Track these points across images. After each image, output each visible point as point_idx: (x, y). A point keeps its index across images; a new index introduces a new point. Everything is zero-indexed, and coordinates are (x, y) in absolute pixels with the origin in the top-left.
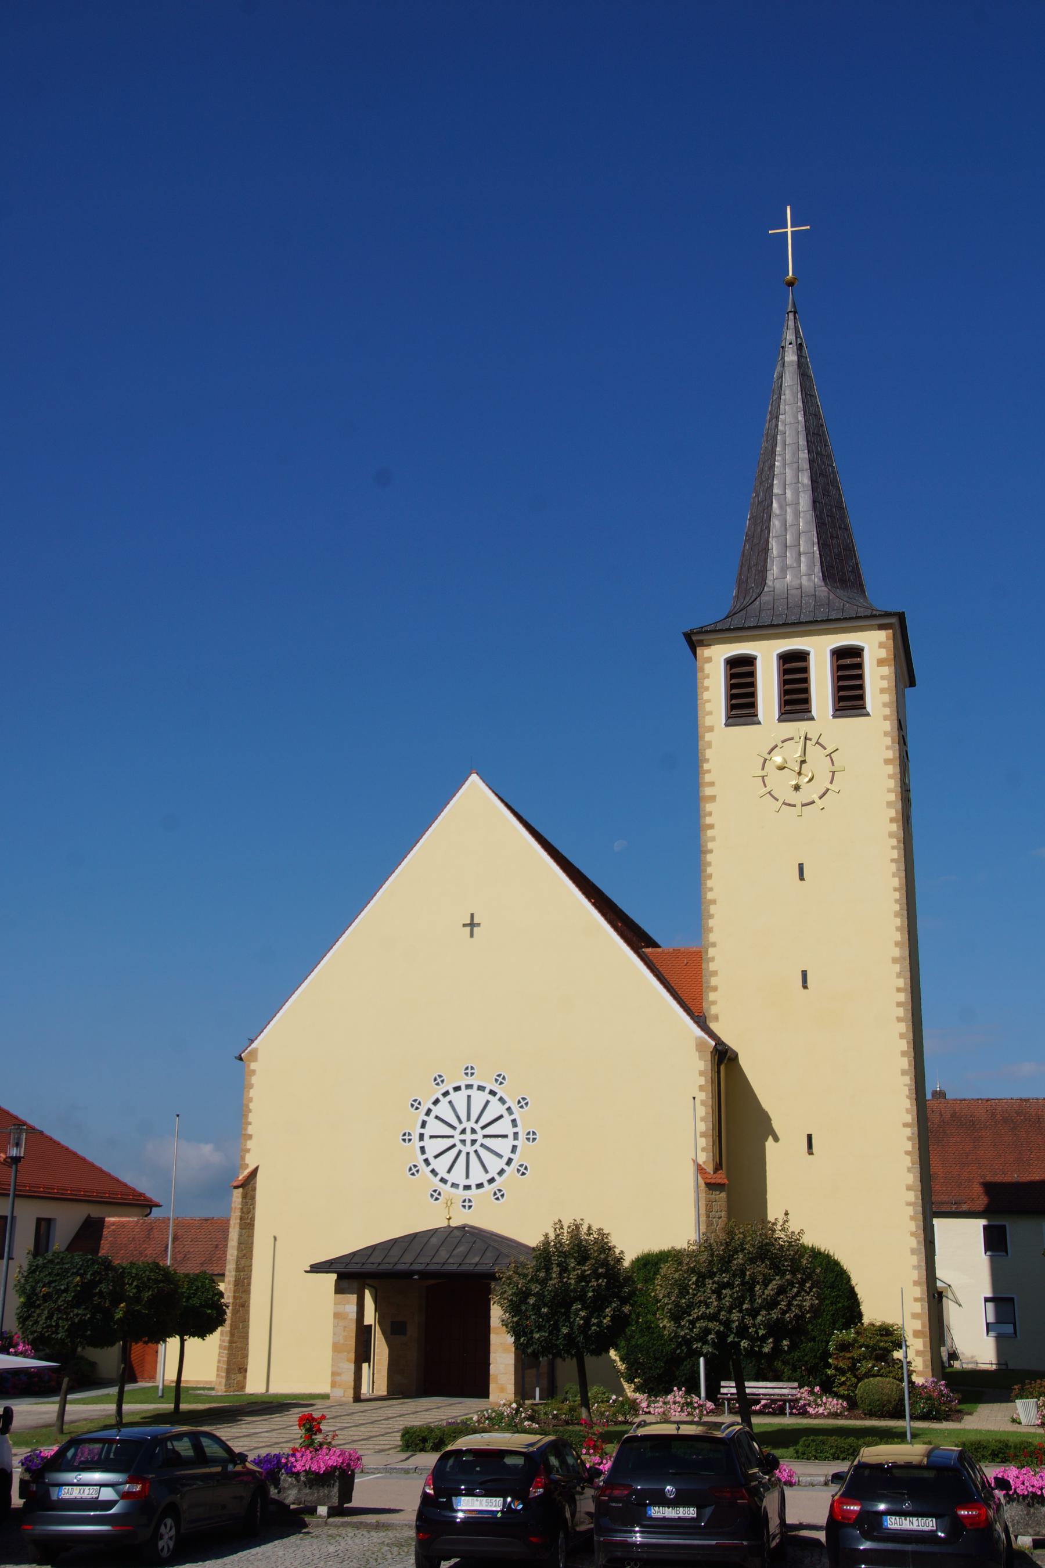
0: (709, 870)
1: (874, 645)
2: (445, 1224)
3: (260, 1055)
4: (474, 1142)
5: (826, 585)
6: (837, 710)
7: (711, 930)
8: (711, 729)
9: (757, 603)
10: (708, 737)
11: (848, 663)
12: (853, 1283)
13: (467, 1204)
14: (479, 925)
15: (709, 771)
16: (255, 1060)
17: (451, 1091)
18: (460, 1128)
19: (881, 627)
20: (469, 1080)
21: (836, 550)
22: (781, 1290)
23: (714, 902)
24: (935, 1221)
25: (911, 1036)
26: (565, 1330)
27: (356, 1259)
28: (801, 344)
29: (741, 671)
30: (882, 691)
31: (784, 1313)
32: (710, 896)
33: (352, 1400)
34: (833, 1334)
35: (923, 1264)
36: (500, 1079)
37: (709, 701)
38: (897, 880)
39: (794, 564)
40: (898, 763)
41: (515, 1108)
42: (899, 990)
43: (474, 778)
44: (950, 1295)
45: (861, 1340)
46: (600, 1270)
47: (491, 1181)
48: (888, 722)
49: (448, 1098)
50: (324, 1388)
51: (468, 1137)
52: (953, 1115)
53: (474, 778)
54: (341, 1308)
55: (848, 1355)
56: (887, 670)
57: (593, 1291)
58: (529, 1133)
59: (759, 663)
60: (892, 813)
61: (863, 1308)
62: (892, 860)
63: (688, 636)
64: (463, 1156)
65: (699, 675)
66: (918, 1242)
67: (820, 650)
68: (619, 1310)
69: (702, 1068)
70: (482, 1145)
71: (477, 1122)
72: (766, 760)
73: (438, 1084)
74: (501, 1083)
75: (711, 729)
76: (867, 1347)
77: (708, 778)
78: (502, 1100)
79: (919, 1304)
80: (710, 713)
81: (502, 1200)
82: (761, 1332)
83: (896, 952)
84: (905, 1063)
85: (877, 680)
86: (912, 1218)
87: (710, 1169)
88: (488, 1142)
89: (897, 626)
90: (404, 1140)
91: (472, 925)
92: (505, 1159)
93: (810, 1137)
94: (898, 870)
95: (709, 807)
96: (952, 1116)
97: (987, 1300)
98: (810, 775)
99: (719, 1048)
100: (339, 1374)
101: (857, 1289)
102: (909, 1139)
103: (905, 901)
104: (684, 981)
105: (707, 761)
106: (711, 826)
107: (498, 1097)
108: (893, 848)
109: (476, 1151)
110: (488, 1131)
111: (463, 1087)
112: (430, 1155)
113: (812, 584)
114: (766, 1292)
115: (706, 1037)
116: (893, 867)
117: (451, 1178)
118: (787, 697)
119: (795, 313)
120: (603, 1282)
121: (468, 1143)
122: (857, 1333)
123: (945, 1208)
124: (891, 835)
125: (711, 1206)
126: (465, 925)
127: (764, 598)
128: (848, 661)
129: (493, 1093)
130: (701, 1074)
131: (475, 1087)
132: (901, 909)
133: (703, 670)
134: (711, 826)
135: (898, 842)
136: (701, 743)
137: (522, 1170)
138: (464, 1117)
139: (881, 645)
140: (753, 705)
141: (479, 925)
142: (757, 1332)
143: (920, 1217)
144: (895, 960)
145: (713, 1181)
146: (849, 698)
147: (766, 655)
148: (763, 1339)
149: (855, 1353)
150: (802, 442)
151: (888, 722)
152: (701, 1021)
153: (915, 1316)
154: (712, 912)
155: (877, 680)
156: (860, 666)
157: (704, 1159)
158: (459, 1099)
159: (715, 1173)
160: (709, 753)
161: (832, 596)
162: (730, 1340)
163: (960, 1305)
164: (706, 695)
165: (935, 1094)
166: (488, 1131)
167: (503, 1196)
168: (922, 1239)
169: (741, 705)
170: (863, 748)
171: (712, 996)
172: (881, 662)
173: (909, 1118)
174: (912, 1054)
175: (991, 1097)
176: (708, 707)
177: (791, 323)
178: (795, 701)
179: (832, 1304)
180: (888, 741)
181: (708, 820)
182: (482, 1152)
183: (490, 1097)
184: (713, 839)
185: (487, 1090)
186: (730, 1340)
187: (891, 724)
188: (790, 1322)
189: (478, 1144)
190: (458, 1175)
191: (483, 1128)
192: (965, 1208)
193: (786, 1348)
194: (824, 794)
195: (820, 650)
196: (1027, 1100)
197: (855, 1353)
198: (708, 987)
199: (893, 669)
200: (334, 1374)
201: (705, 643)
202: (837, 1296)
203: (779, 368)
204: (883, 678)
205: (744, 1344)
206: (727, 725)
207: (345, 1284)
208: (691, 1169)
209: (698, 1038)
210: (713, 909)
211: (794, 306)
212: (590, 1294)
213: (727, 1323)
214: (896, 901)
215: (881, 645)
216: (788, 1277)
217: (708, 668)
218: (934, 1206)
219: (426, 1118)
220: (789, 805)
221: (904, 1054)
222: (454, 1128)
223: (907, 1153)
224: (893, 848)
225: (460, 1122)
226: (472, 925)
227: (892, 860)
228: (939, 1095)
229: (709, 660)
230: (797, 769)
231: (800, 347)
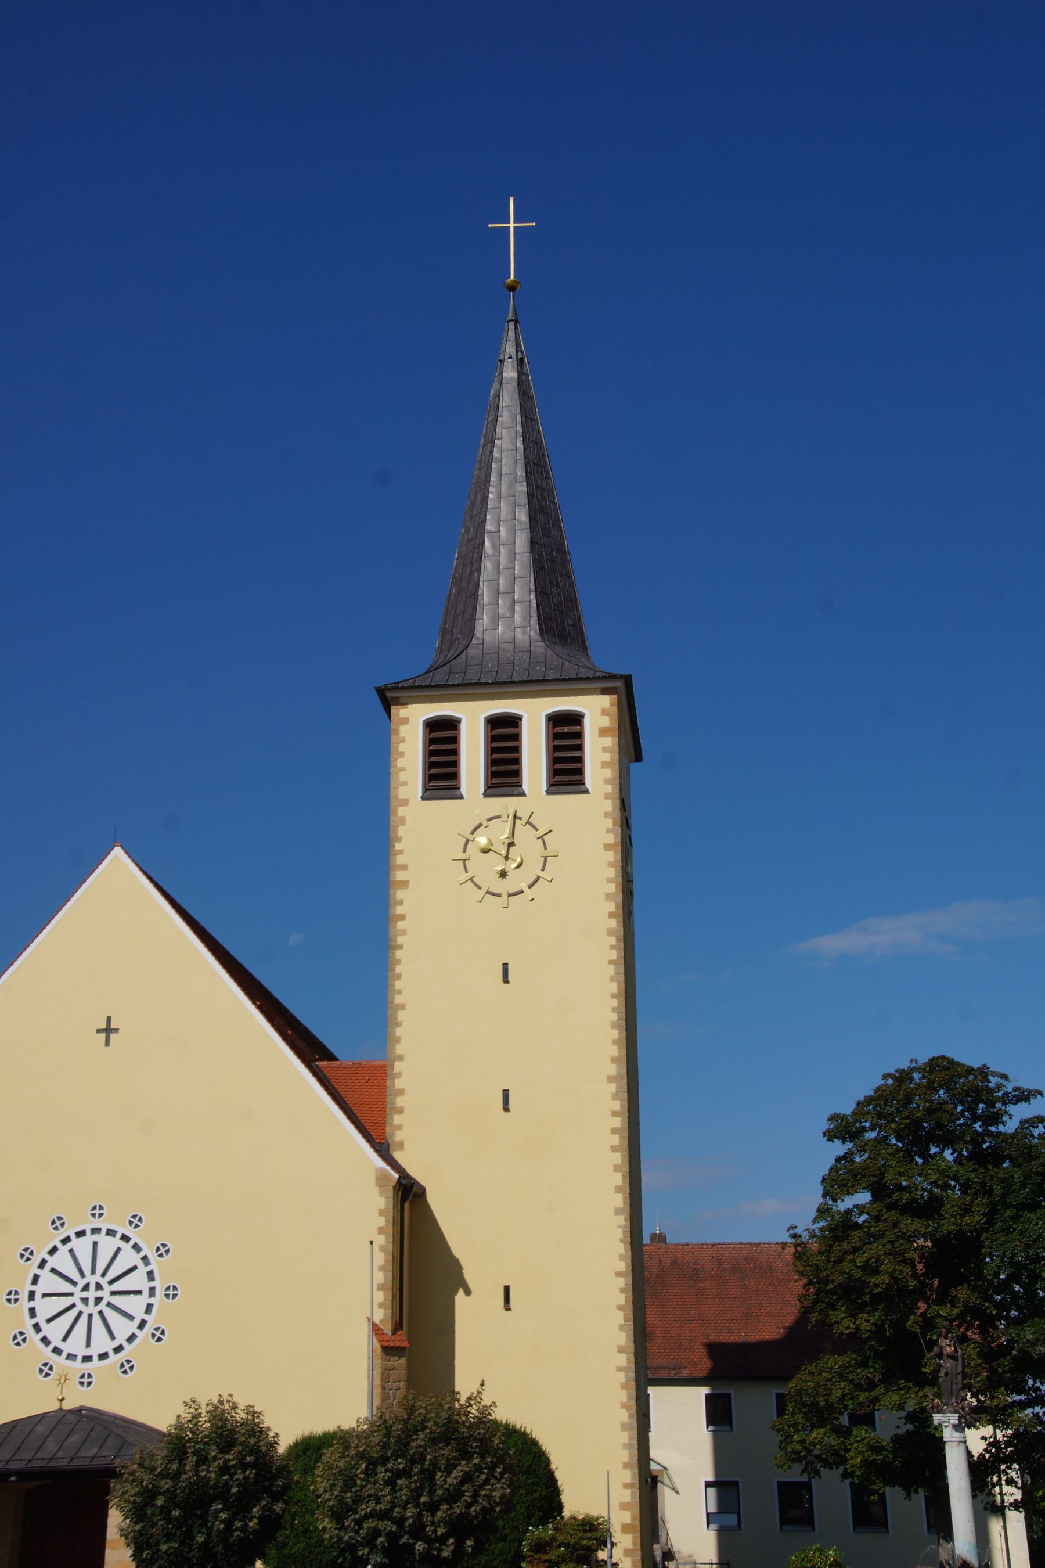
0: (398, 969)
1: (596, 711)
2: (56, 1407)
4: (98, 1300)
5: (543, 640)
6: (551, 785)
8: (405, 802)
9: (463, 657)
10: (401, 811)
11: (565, 731)
12: (553, 1466)
13: (85, 1380)
14: (116, 1030)
15: (401, 852)
17: (73, 1237)
18: (82, 1283)
19: (604, 691)
20: (96, 1223)
21: (555, 600)
22: (467, 1478)
23: (402, 1007)
24: (651, 1390)
25: (626, 1168)
26: (200, 1539)
28: (522, 359)
29: (442, 736)
30: (604, 765)
31: (469, 1506)
32: (398, 1000)
34: (527, 1531)
35: (635, 1442)
36: (136, 1221)
37: (403, 769)
38: (615, 984)
39: (507, 614)
40: (619, 848)
41: (152, 1257)
42: (614, 1114)
43: (118, 851)
44: (666, 1480)
45: (561, 1538)
46: (249, 1459)
48: (610, 801)
49: (69, 1246)
51: (92, 1294)
52: (674, 1263)
53: (118, 851)
55: (545, 1557)
56: (610, 741)
57: (238, 1486)
58: (168, 1288)
59: (464, 728)
60: (612, 907)
61: (565, 1498)
62: (611, 962)
63: (381, 692)
64: (84, 1319)
65: (393, 738)
66: (630, 1416)
67: (534, 713)
68: (269, 1509)
69: (383, 1206)
70: (109, 1304)
71: (103, 1275)
72: (468, 841)
73: (56, 1228)
74: (137, 1226)
75: (405, 802)
76: (567, 1546)
77: (399, 860)
78: (136, 1247)
79: (629, 1492)
80: (405, 784)
81: (130, 1374)
82: (441, 1531)
83: (613, 1069)
84: (619, 1200)
85: (598, 751)
86: (624, 1386)
87: (388, 1329)
88: (117, 1300)
89: (623, 690)
90: (9, 1300)
91: (108, 1030)
92: (137, 1322)
93: (507, 1289)
94: (617, 973)
95: (400, 894)
96: (672, 1264)
97: (708, 1485)
98: (519, 860)
99: (404, 1182)
101: (557, 1475)
102: (622, 1290)
103: (624, 1010)
104: (363, 1098)
105: (400, 840)
106: (402, 917)
107: (132, 1243)
108: (612, 947)
109: (101, 1312)
110: (118, 1286)
111: (88, 1232)
112: (41, 1318)
113: (527, 638)
114: (448, 1480)
115: (388, 1168)
116: (611, 970)
117: (67, 1348)
118: (494, 768)
119: (516, 322)
120: (251, 1473)
121: (92, 1301)
122: (556, 1529)
123: (663, 1374)
124: (610, 932)
125: (388, 1375)
126: (99, 1031)
127: (472, 652)
128: (566, 729)
129: (125, 1238)
130: (381, 1213)
131: (104, 1231)
132: (619, 1019)
133: (397, 733)
134: (402, 917)
135: (618, 940)
136: (393, 819)
137: (158, 1334)
138: (87, 1270)
139: (604, 712)
140: (455, 776)
141: (116, 1030)
142: (435, 1531)
143: (633, 1384)
144: (610, 1079)
145: (391, 1344)
146: (566, 773)
147: (472, 717)
148: (442, 1540)
149: (553, 1555)
150: (521, 472)
151: (610, 801)
152: (383, 1148)
153: (624, 1506)
154: (400, 1019)
155: (598, 751)
156: (579, 735)
157: (381, 1317)
158: (82, 1247)
159: (393, 1333)
160: (401, 831)
161: (550, 653)
162: (403, 1541)
163: (677, 1492)
164: (400, 763)
165: (654, 1237)
166: (118, 1286)
167: (132, 1368)
168: (634, 1411)
170: (582, 828)
171: (397, 1119)
172: (603, 732)
173: (623, 1266)
174: (628, 1190)
175: (717, 1241)
176: (403, 776)
177: (511, 334)
178: (504, 774)
179: (527, 1493)
180: (609, 823)
181: (399, 910)
182: (109, 1313)
183: (122, 1244)
184: (404, 932)
185: (119, 1235)
186: (403, 1541)
187: (613, 803)
188: (476, 1517)
189: (104, 1302)
190: (76, 1344)
191: (111, 1282)
192: (685, 1373)
193: (470, 1550)
194: (535, 882)
195: (534, 713)
196: (758, 1245)
197: (553, 1555)
198: (393, 1108)
201: (401, 701)
202: (534, 1484)
203: (495, 386)
204: (605, 750)
205: (419, 1547)
206: (424, 798)
208: (365, 1329)
209: (381, 1169)
210: (401, 1015)
211: (515, 314)
212: (234, 1490)
213: (400, 1522)
214: (614, 1010)
215: (604, 712)
216: (476, 1461)
217: (403, 730)
218: (649, 1371)
219: (39, 1272)
220: (494, 894)
221: (618, 1189)
222: (74, 1283)
223: (620, 1308)
224: (612, 947)
225: (83, 1275)
226: (108, 1030)
227: (611, 962)
228: (659, 1239)
229: (405, 721)
230: (504, 852)
231: (521, 362)
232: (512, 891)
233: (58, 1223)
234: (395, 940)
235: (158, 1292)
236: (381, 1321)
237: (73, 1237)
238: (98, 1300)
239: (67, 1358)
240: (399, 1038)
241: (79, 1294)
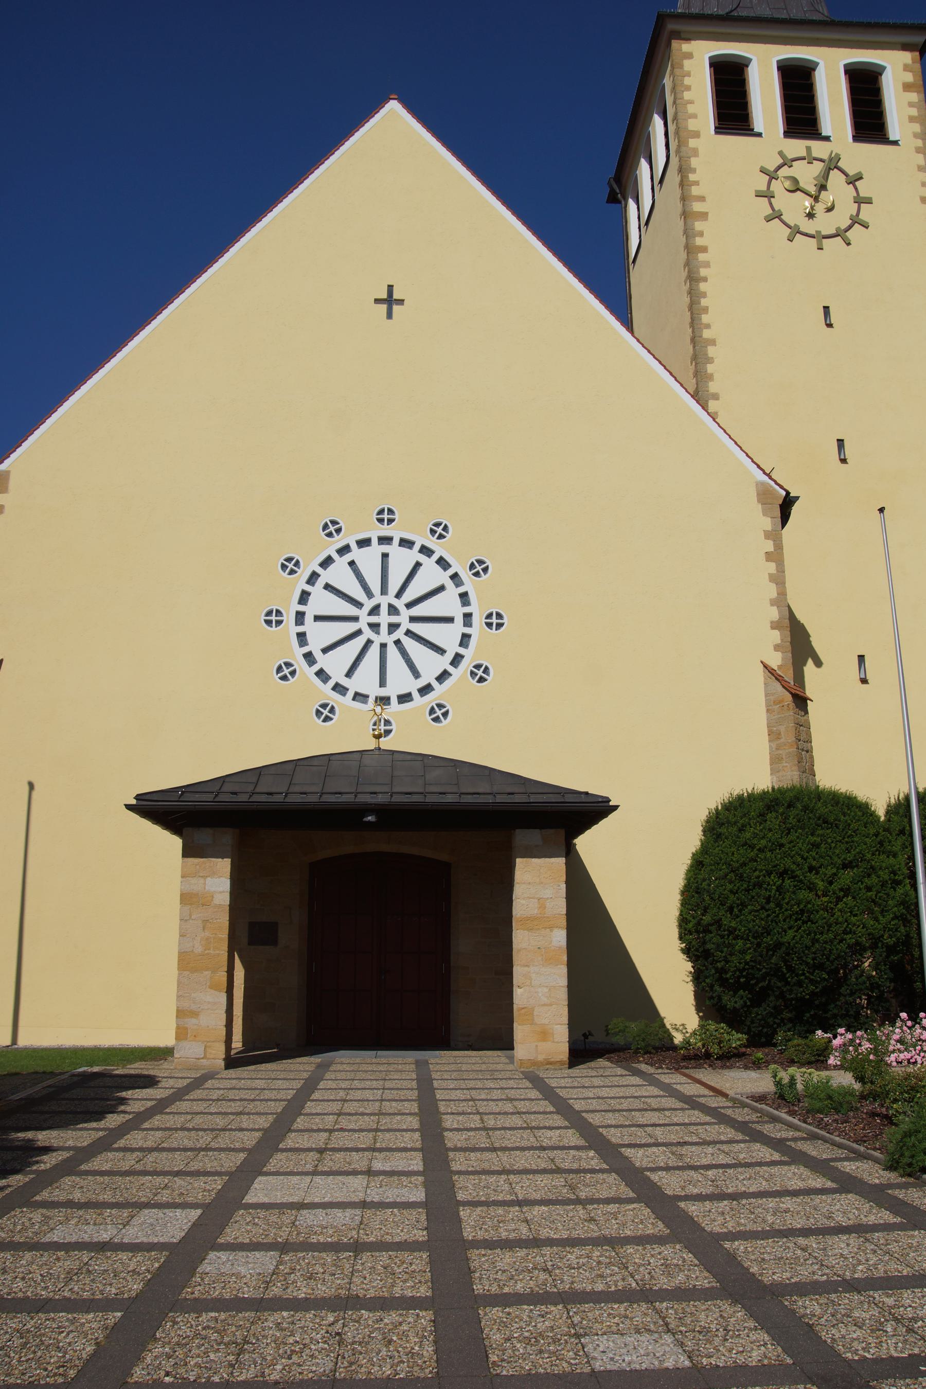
2: (371, 744)
7: (711, 377)
8: (696, 135)
11: (864, 87)
14: (401, 302)
18: (369, 605)
27: (228, 788)
29: (730, 80)
33: (222, 1064)
43: (394, 106)
50: (166, 1039)
53: (394, 106)
54: (196, 885)
70: (408, 633)
80: (694, 116)
91: (390, 301)
100: (194, 1014)
105: (694, 171)
107: (435, 557)
121: (384, 629)
126: (377, 301)
138: (375, 587)
141: (401, 302)
154: (710, 355)
157: (779, 663)
169: (733, 114)
184: (707, 265)
185: (417, 547)
195: (830, 68)
199: (922, 96)
200: (181, 1013)
207: (204, 836)
208: (759, 674)
209: (763, 484)
222: (359, 605)
232: (824, 233)
233: (332, 528)
234: (698, 272)
236: (780, 667)
237: (354, 546)
239: (354, 699)
240: (712, 375)
241: (384, 601)
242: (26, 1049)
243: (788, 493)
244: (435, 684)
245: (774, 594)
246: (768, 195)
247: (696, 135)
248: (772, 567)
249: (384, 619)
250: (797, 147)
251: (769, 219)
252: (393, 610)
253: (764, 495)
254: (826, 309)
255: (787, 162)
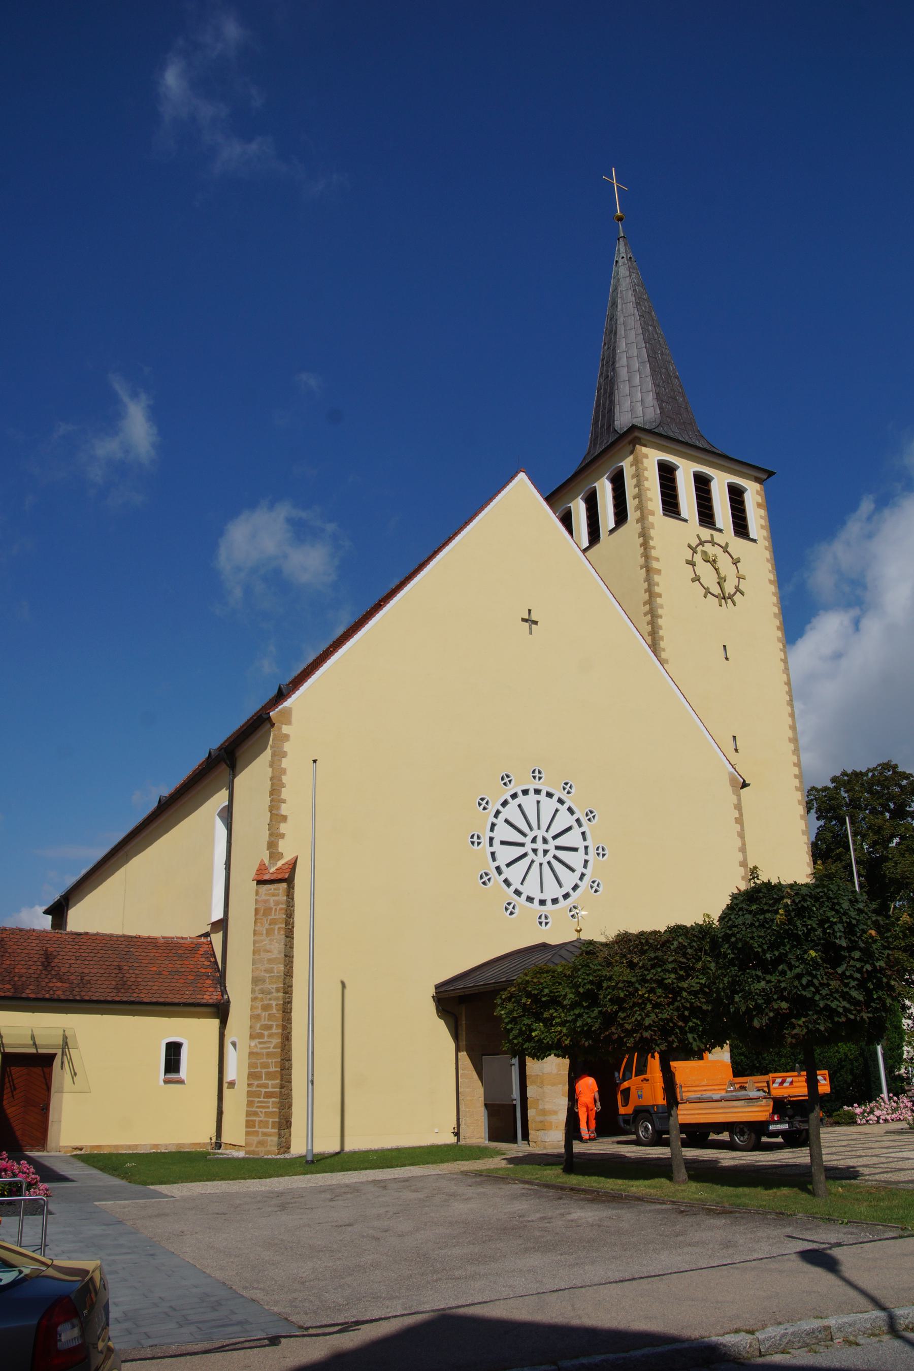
2: (573, 937)
3: (295, 717)
16: (289, 723)
29: (667, 473)
43: (522, 476)
47: (566, 896)
53: (522, 476)
121: (540, 853)
209: (731, 774)
222: (525, 835)
229: (646, 456)
233: (506, 780)
235: (590, 850)
238: (535, 851)
242: (353, 1153)
243: (744, 781)
244: (571, 892)
245: (740, 845)
246: (692, 563)
247: (653, 513)
248: (738, 827)
249: (540, 845)
250: (706, 533)
251: (693, 580)
252: (545, 841)
253: (733, 780)
254: (725, 646)
255: (702, 543)
